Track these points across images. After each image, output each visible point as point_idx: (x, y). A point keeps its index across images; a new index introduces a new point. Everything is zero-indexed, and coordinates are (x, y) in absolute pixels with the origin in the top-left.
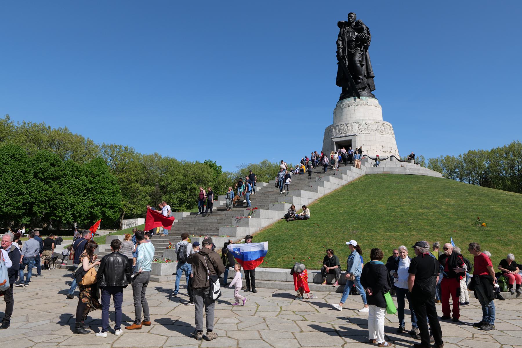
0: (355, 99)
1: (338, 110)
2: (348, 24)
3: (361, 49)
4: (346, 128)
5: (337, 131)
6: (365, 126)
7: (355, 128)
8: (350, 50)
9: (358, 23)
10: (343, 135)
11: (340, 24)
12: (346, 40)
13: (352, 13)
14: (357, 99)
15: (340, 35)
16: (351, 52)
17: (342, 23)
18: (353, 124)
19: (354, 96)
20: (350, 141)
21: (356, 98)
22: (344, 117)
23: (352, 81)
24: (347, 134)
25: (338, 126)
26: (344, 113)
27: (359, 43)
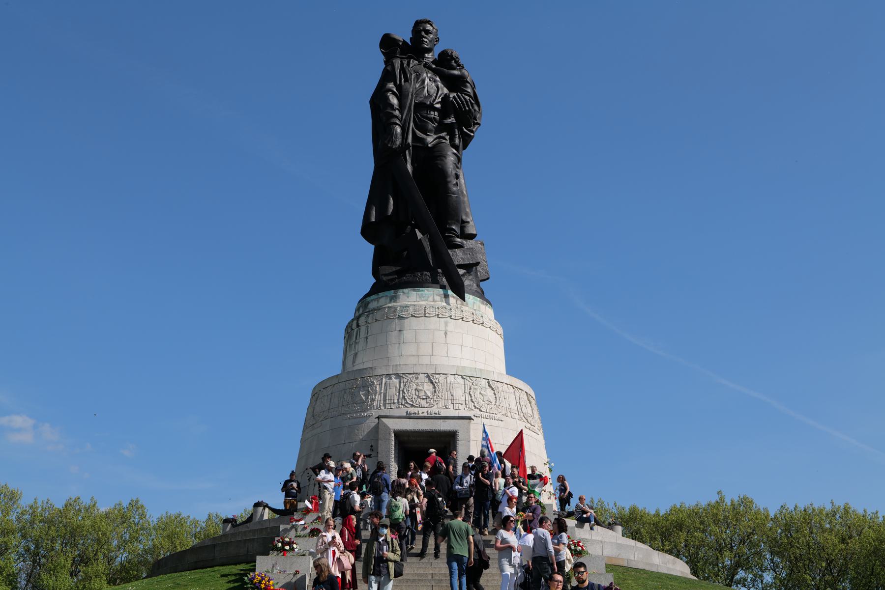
0: (446, 296)
1: (365, 322)
2: (416, 48)
3: (452, 140)
4: (428, 388)
5: (393, 393)
6: (489, 392)
7: (459, 394)
8: (418, 133)
9: (446, 60)
10: (422, 412)
11: (388, 44)
12: (411, 101)
13: (428, 22)
14: (453, 299)
15: (388, 75)
16: (422, 141)
17: (395, 41)
18: (450, 379)
19: (443, 287)
21: (450, 292)
22: (409, 350)
23: (415, 233)
24: (434, 410)
25: (398, 376)
26: (408, 335)
27: (451, 120)
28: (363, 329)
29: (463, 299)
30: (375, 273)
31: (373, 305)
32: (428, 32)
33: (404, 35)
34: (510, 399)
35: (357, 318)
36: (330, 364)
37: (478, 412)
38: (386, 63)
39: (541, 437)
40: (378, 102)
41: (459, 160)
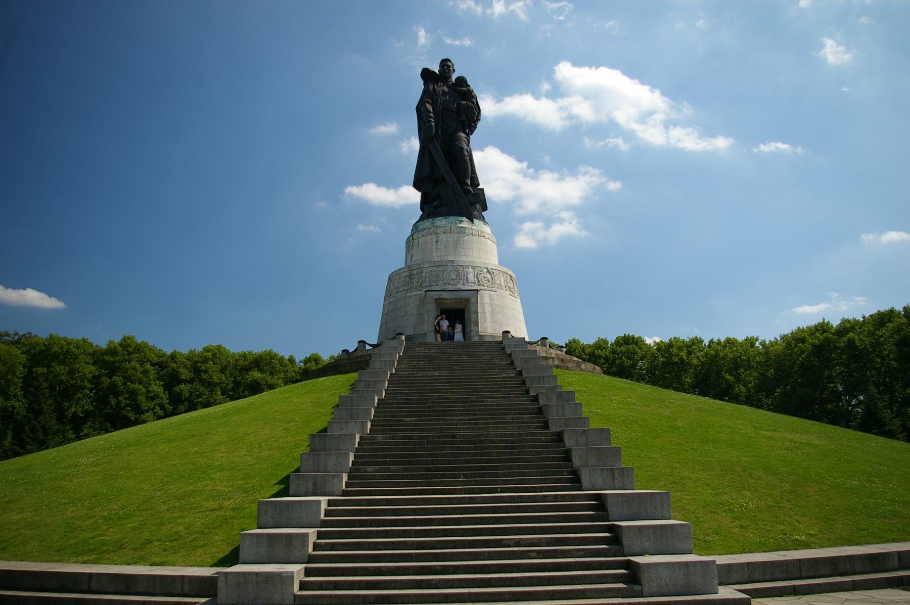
6: (489, 276)
7: (471, 277)
11: (426, 74)
20: (467, 301)
28: (416, 241)
29: (472, 222)
30: (422, 209)
31: (421, 227)
32: (449, 66)
33: (436, 69)
34: (500, 279)
35: (412, 235)
36: (398, 260)
37: (482, 287)
38: (424, 84)
39: (518, 300)
40: (420, 109)
41: (469, 141)
